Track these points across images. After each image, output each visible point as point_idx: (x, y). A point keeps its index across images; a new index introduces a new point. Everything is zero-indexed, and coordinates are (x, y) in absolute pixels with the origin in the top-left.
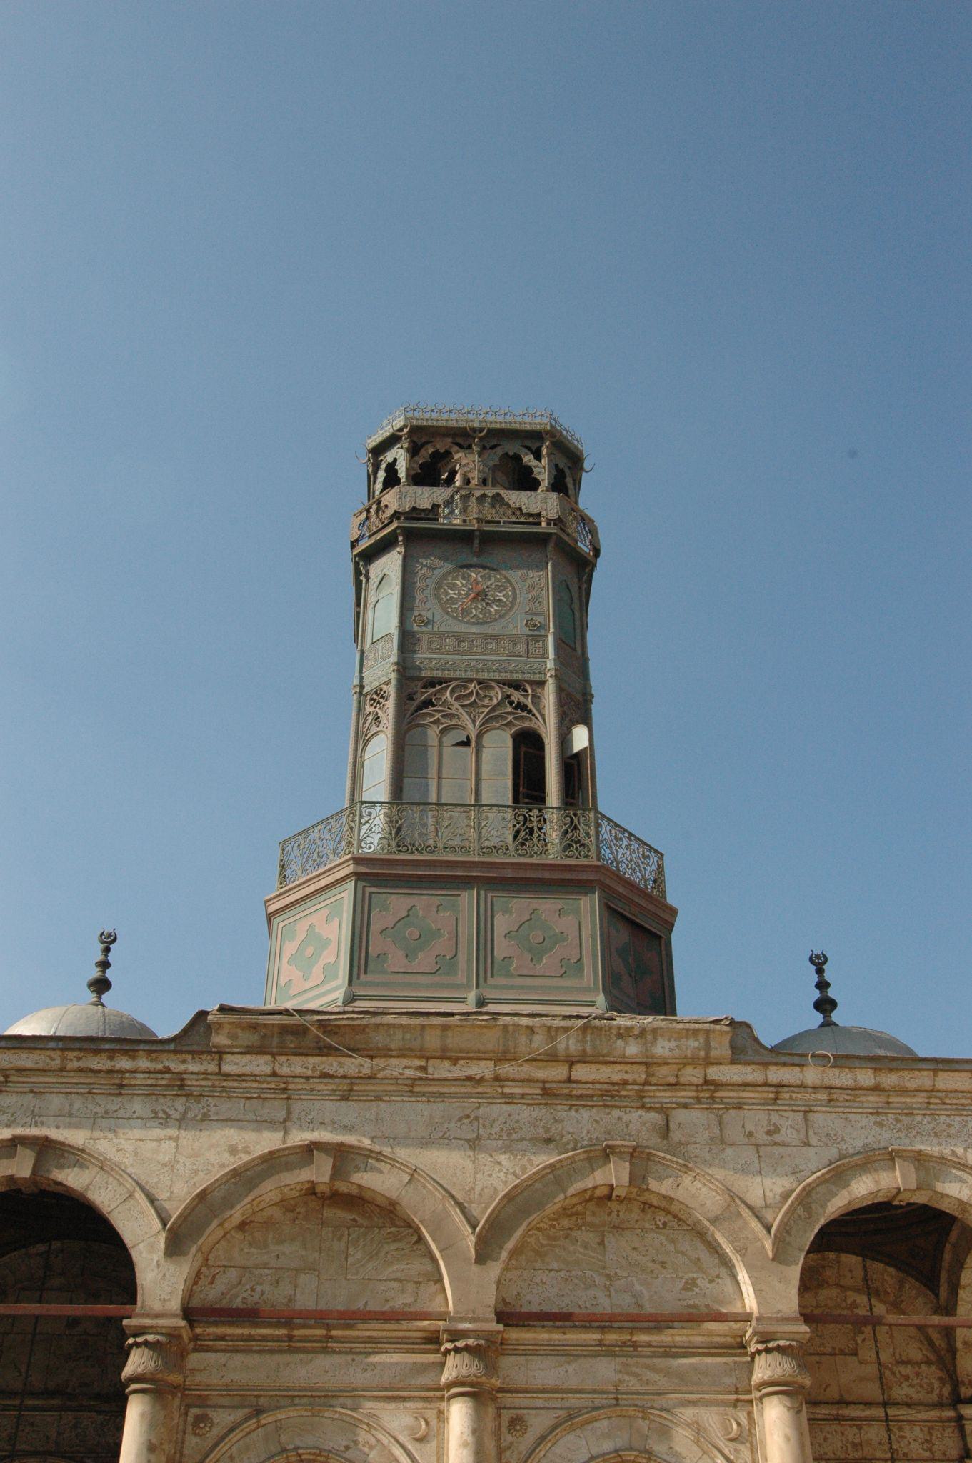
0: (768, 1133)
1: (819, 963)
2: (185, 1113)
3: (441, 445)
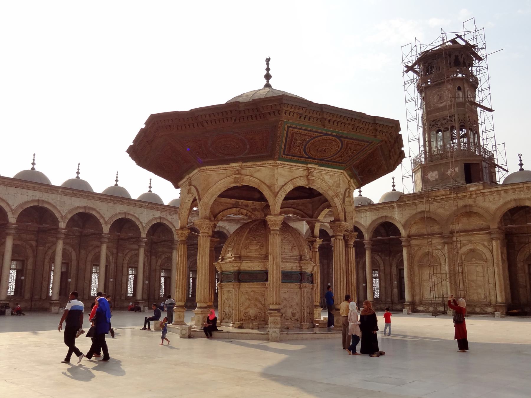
1: (520, 156)
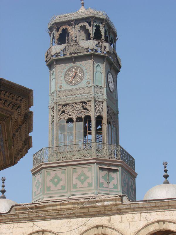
2: (14, 227)
3: (64, 27)
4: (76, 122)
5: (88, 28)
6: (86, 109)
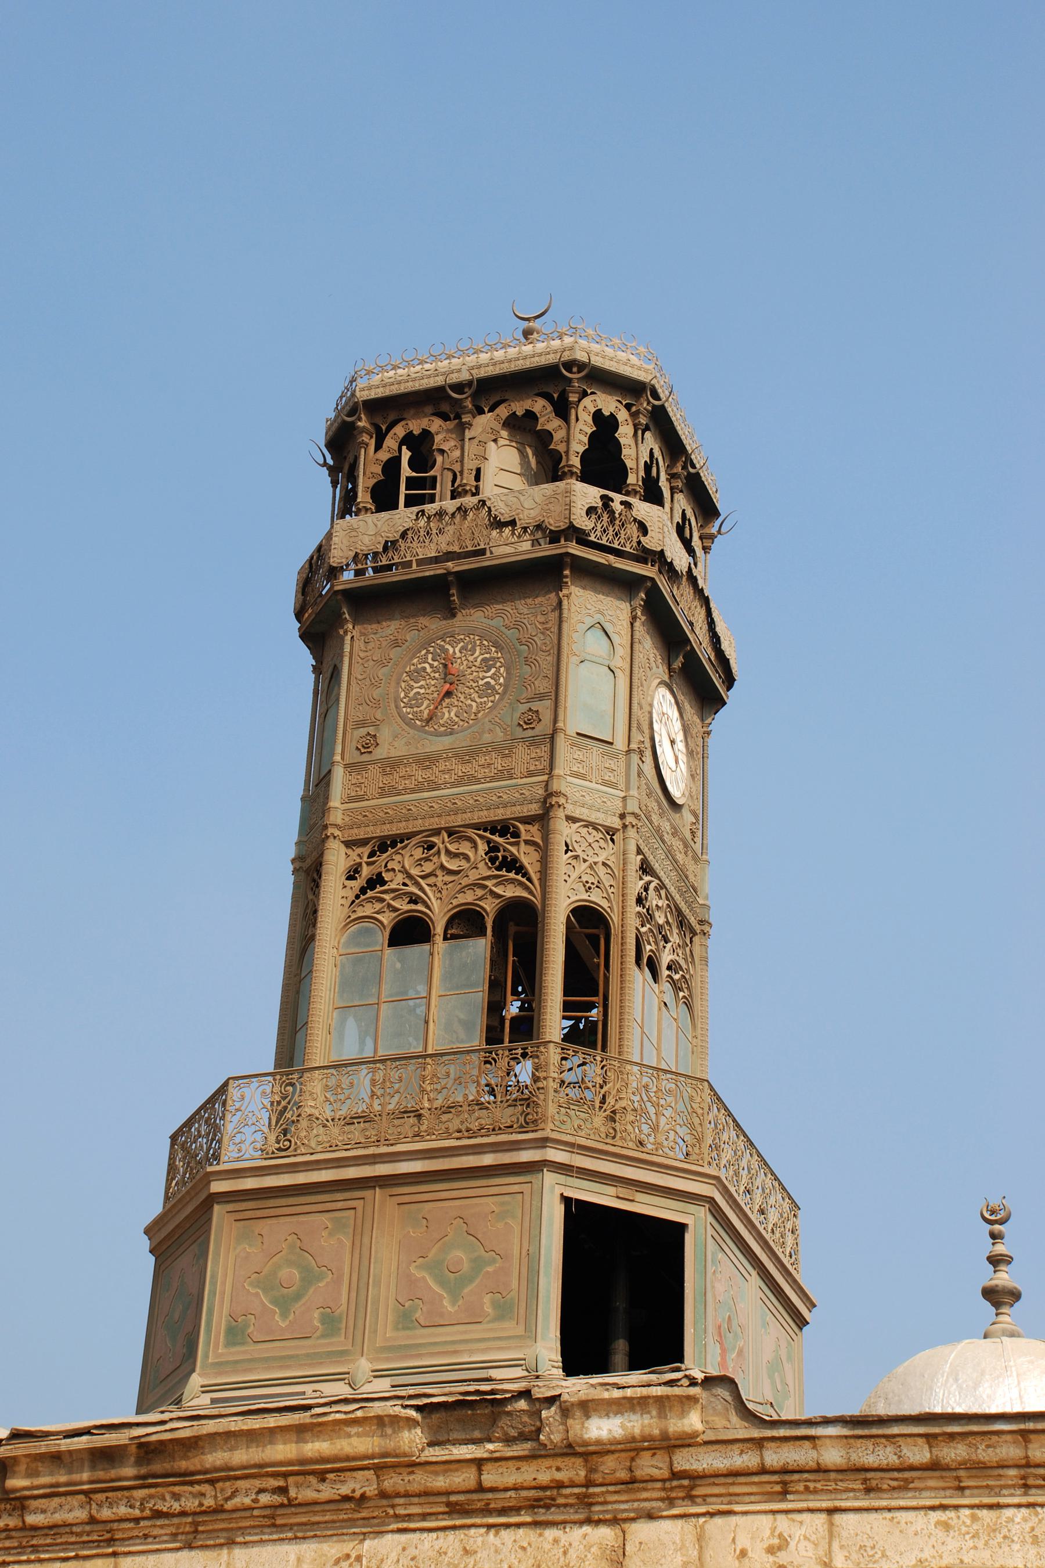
0: (771, 1550)
4: (445, 939)
5: (549, 427)
6: (513, 865)
